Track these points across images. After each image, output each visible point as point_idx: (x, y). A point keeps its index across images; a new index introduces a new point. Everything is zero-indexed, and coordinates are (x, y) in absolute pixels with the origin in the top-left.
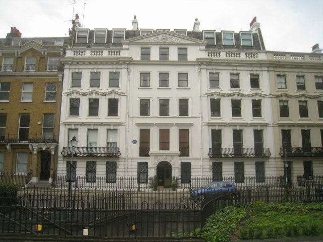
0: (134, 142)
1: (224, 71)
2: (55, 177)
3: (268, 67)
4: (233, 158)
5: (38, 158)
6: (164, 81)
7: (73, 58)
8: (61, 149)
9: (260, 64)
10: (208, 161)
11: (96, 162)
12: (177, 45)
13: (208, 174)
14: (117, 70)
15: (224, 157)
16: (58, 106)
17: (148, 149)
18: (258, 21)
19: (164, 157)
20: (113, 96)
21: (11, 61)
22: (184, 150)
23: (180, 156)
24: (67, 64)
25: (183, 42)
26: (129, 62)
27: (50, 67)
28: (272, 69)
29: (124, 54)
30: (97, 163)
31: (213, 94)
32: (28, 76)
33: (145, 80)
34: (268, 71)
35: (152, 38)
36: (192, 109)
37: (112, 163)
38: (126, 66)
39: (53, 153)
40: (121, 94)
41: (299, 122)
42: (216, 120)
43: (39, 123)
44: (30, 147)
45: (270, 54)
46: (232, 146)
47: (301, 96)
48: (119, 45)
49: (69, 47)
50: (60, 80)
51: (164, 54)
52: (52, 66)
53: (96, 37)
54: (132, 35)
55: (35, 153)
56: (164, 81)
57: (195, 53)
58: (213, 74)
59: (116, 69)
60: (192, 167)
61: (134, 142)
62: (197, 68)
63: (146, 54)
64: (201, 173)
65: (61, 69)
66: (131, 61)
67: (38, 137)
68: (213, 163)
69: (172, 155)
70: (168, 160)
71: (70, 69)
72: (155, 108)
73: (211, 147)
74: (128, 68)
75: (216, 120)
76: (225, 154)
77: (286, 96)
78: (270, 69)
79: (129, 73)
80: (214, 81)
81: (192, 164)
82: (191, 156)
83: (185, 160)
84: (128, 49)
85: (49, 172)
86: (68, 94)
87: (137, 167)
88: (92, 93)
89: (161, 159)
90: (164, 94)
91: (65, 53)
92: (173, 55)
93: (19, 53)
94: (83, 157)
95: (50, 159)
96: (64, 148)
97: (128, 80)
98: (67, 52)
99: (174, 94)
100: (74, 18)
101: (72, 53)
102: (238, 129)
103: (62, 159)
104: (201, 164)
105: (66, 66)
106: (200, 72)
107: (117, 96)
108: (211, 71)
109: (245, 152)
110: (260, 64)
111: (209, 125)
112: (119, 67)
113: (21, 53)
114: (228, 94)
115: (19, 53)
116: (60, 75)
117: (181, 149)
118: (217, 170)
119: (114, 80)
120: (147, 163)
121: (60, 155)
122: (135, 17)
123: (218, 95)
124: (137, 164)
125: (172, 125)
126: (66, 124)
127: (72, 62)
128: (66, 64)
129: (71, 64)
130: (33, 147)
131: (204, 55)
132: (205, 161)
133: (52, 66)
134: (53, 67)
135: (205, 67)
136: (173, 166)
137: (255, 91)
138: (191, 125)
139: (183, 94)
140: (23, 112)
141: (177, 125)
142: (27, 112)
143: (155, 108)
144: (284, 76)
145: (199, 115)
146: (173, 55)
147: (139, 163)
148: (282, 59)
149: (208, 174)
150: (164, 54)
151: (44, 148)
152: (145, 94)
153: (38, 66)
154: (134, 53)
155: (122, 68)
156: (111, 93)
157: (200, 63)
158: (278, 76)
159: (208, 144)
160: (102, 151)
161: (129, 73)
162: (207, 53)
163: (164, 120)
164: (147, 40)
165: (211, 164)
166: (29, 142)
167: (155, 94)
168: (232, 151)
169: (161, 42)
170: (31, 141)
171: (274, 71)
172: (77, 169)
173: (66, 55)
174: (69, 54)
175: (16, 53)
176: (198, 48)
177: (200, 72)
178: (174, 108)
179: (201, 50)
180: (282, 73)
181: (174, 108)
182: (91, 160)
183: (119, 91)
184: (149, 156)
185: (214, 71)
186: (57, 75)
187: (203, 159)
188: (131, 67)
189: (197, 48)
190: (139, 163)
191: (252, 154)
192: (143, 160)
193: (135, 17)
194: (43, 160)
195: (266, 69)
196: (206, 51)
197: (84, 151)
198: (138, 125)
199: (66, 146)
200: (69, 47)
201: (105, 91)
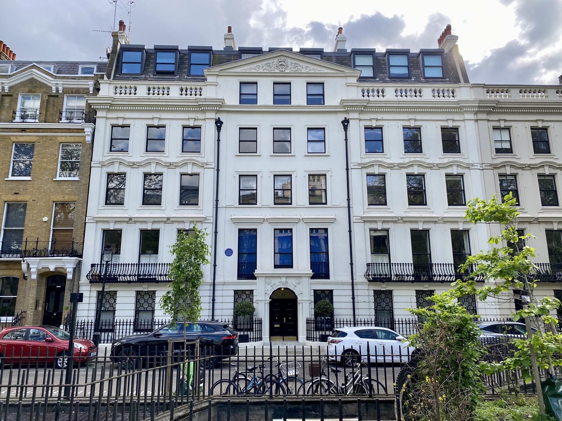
0: (229, 252)
2: (71, 321)
3: (476, 113)
4: (412, 282)
5: (39, 285)
7: (114, 99)
8: (86, 269)
9: (459, 108)
10: (366, 287)
11: (115, 292)
14: (198, 123)
15: (396, 281)
17: (254, 266)
18: (453, 32)
19: (283, 280)
23: (313, 278)
27: (69, 115)
28: (484, 116)
30: (118, 294)
32: (23, 130)
34: (477, 120)
35: (260, 64)
37: (147, 293)
39: (70, 276)
41: (541, 215)
43: (45, 219)
44: (24, 266)
45: (481, 90)
46: (410, 259)
47: (543, 166)
49: (105, 78)
50: (88, 139)
52: (71, 113)
55: (34, 277)
58: (372, 128)
61: (229, 252)
66: (221, 106)
67: (41, 246)
69: (299, 276)
70: (291, 284)
76: (397, 275)
77: (512, 166)
78: (481, 116)
83: (321, 285)
85: (61, 314)
86: (103, 165)
87: (232, 299)
89: (278, 284)
94: (129, 282)
95: (63, 289)
96: (93, 265)
98: (101, 86)
100: (117, 29)
101: (112, 90)
102: (421, 228)
103: (88, 288)
105: (99, 114)
108: (368, 123)
109: (436, 270)
110: (461, 108)
112: (201, 116)
114: (398, 164)
116: (88, 130)
117: (314, 265)
120: (252, 291)
121: (84, 279)
122: (230, 29)
124: (232, 293)
125: (298, 221)
126: (98, 221)
127: (111, 107)
129: (108, 110)
130: (28, 265)
131: (355, 94)
133: (71, 113)
134: (75, 115)
136: (299, 298)
137: (450, 157)
138: (333, 221)
140: (12, 198)
142: (19, 198)
144: (508, 129)
147: (236, 292)
148: (502, 97)
151: (52, 268)
153: (44, 112)
155: (205, 119)
158: (495, 128)
160: (166, 270)
162: (360, 89)
163: (282, 213)
166: (21, 257)
168: (410, 270)
169: (277, 71)
170: (25, 254)
171: (488, 121)
172: (117, 307)
173: (101, 93)
176: (343, 81)
179: (348, 85)
180: (502, 124)
182: (145, 288)
184: (255, 278)
185: (374, 124)
189: (342, 81)
190: (236, 292)
191: (451, 276)
192: (245, 285)
193: (230, 29)
194: (49, 290)
195: (471, 116)
197: (134, 270)
198: (235, 221)
199: (98, 261)
200: (105, 78)
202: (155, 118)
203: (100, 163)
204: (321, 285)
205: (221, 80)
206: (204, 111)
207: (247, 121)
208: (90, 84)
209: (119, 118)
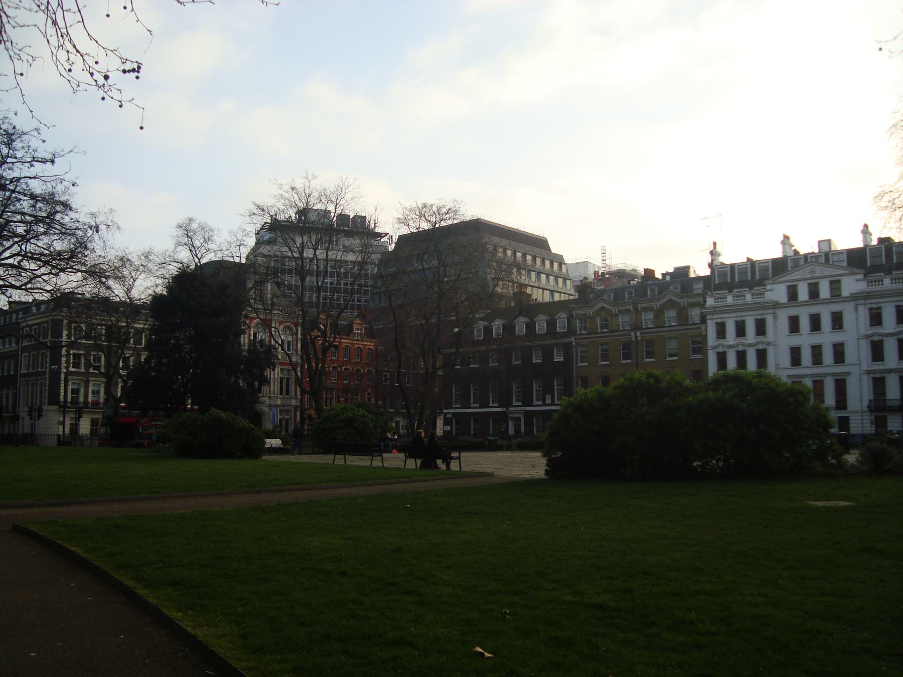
1: (887, 304)
6: (815, 323)
12: (827, 277)
13: (869, 429)
16: (704, 362)
20: (761, 347)
21: (650, 316)
22: (841, 403)
24: (710, 314)
25: (839, 273)
26: (776, 305)
29: (769, 296)
31: (873, 335)
33: (794, 325)
36: (850, 354)
38: (771, 311)
40: (769, 344)
42: (878, 366)
48: (761, 283)
51: (814, 293)
53: (739, 273)
54: (779, 267)
56: (815, 323)
57: (852, 285)
59: (762, 314)
60: (851, 422)
62: (852, 304)
63: (793, 294)
64: (860, 429)
65: (704, 320)
68: (876, 417)
71: (712, 319)
72: (806, 357)
73: (872, 398)
74: (773, 313)
75: (878, 366)
79: (775, 318)
80: (876, 318)
81: (851, 418)
82: (849, 408)
83: (842, 414)
84: (771, 290)
86: (714, 348)
88: (738, 345)
90: (816, 339)
91: (705, 301)
92: (825, 291)
93: (658, 306)
97: (775, 327)
99: (827, 338)
104: (860, 418)
105: (708, 317)
106: (856, 310)
107: (765, 347)
111: (869, 372)
112: (764, 312)
113: (660, 306)
115: (658, 306)
117: (837, 401)
118: (880, 423)
119: (761, 328)
123: (879, 335)
125: (826, 375)
127: (714, 311)
128: (708, 314)
132: (864, 414)
135: (862, 302)
138: (848, 374)
139: (838, 337)
141: (832, 374)
143: (806, 357)
145: (856, 362)
146: (825, 291)
149: (869, 429)
150: (814, 293)
152: (795, 341)
154: (777, 292)
156: (758, 343)
157: (856, 297)
159: (867, 394)
161: (775, 318)
162: (865, 282)
164: (793, 276)
165: (873, 418)
167: (805, 339)
169: (809, 276)
174: (710, 302)
175: (655, 306)
177: (856, 310)
178: (828, 356)
179: (857, 280)
181: (828, 356)
183: (767, 340)
186: (700, 328)
187: (863, 412)
188: (778, 311)
196: (864, 280)
201: (752, 342)
202: (738, 316)
203: (712, 347)
204: (842, 414)
205: (775, 286)
206: (766, 309)
207: (793, 312)
208: (701, 299)
209: (719, 318)
